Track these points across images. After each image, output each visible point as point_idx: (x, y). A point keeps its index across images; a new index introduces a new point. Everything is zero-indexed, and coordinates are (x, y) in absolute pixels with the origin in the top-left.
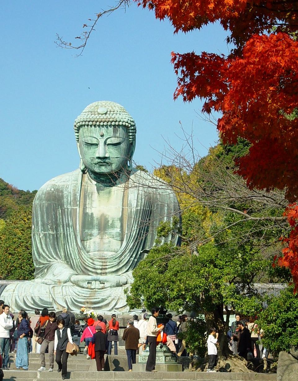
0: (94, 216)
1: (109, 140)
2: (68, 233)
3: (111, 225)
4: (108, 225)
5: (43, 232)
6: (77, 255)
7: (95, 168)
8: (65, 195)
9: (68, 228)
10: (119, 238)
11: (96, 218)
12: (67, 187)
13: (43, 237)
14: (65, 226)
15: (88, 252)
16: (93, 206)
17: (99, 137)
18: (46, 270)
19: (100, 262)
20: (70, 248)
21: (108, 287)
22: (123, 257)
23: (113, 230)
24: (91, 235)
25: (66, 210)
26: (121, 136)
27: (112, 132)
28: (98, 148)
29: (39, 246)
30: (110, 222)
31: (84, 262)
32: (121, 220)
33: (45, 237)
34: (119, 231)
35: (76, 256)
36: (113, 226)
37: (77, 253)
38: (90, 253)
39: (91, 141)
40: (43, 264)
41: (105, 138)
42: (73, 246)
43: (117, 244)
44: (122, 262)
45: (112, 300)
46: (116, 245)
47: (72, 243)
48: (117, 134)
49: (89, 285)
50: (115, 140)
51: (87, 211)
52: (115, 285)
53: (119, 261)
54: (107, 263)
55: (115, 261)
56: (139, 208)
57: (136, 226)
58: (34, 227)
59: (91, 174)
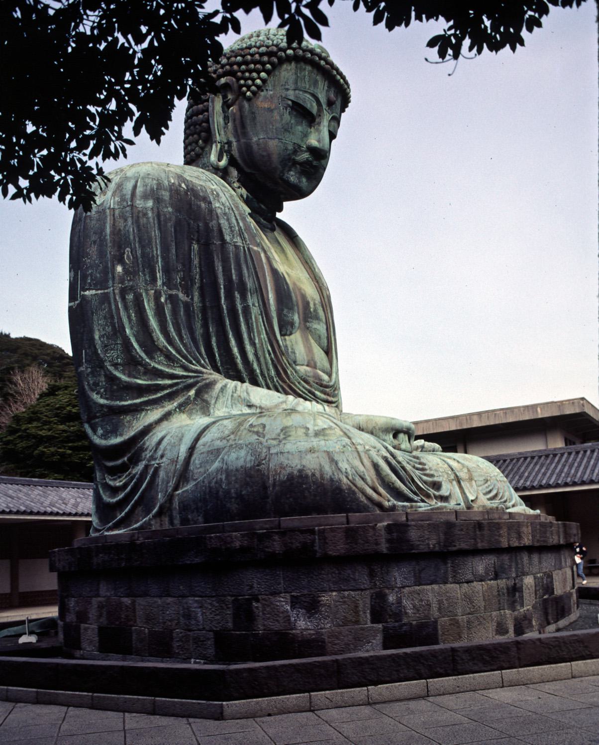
2: (239, 307)
4: (311, 312)
5: (165, 288)
6: (271, 367)
7: (292, 173)
8: (219, 211)
9: (237, 295)
12: (215, 193)
13: (166, 301)
14: (222, 287)
15: (295, 362)
17: (324, 106)
18: (192, 393)
19: (322, 392)
20: (249, 348)
24: (292, 324)
25: (231, 248)
28: (312, 130)
29: (153, 323)
30: (312, 305)
31: (293, 386)
33: (172, 303)
35: (268, 370)
37: (270, 362)
38: (298, 368)
39: (312, 105)
40: (172, 376)
42: (257, 341)
47: (256, 334)
49: (396, 442)
58: (124, 269)
59: (239, 188)
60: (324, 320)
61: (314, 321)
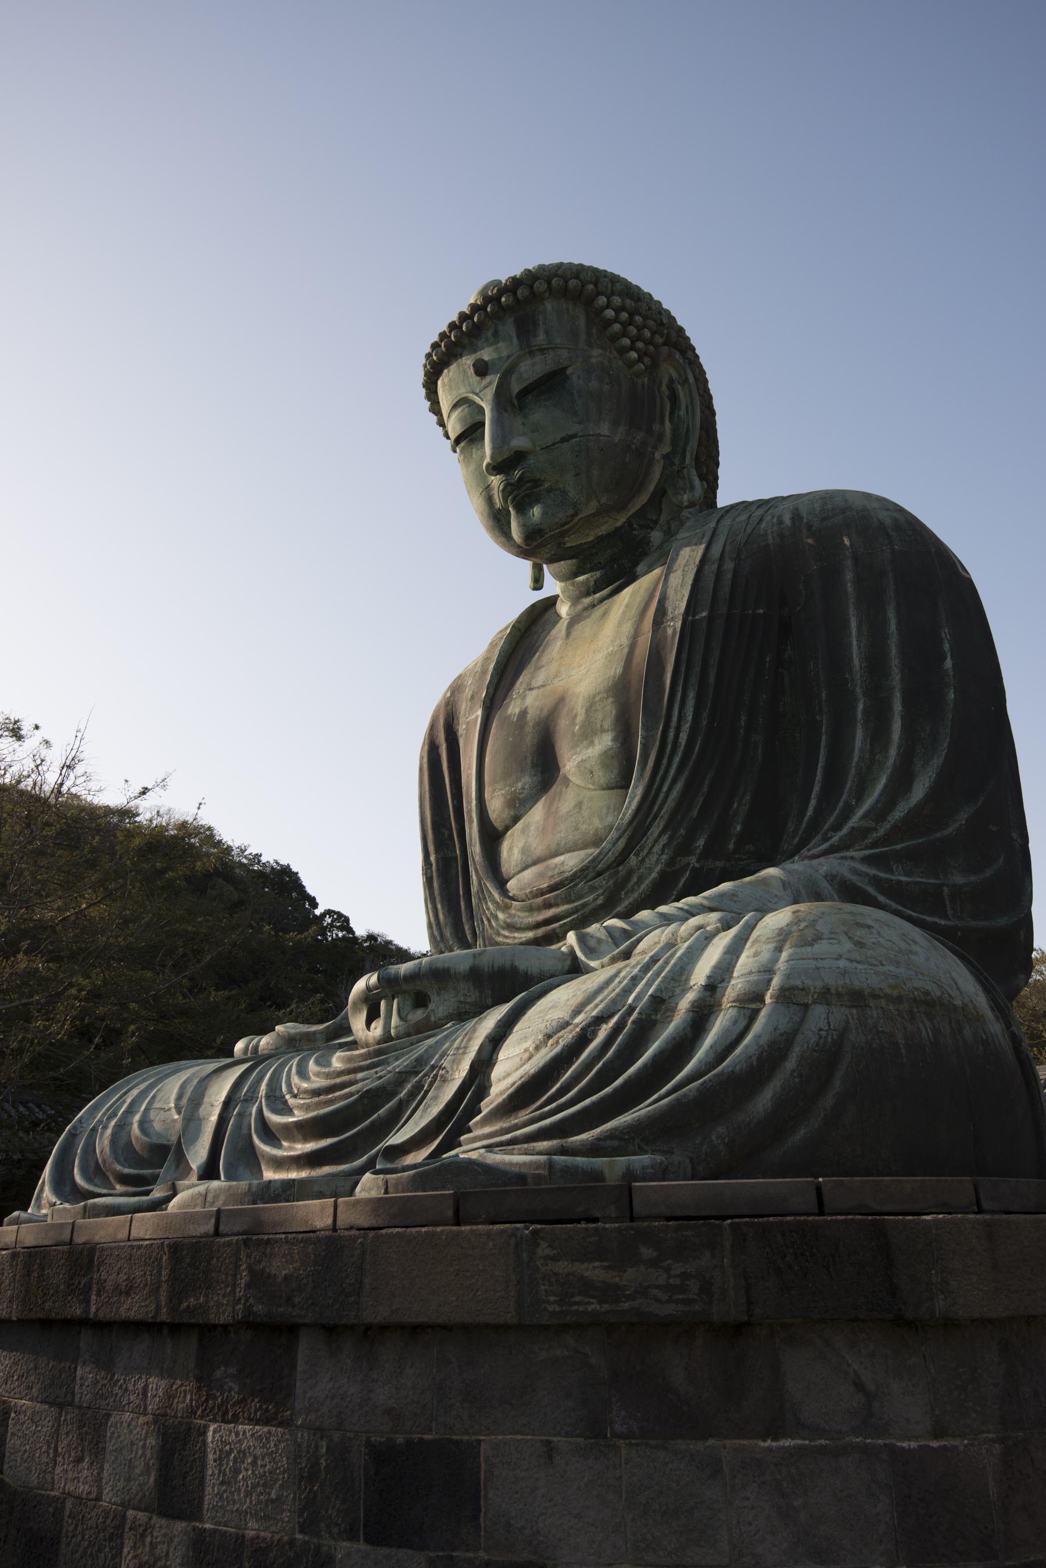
0: (529, 717)
1: (514, 378)
3: (580, 728)
10: (613, 775)
11: (531, 724)
16: (534, 684)
21: (449, 1018)
22: (633, 860)
23: (587, 748)
26: (558, 341)
27: (515, 340)
32: (620, 689)
34: (610, 743)
36: (588, 734)
41: (494, 379)
43: (609, 808)
44: (630, 885)
45: (412, 1095)
46: (604, 811)
48: (536, 336)
50: (531, 369)
51: (509, 711)
52: (489, 1001)
53: (611, 882)
54: (557, 905)
55: (593, 889)
56: (704, 614)
57: (691, 695)
60: (608, 723)
61: (578, 749)
